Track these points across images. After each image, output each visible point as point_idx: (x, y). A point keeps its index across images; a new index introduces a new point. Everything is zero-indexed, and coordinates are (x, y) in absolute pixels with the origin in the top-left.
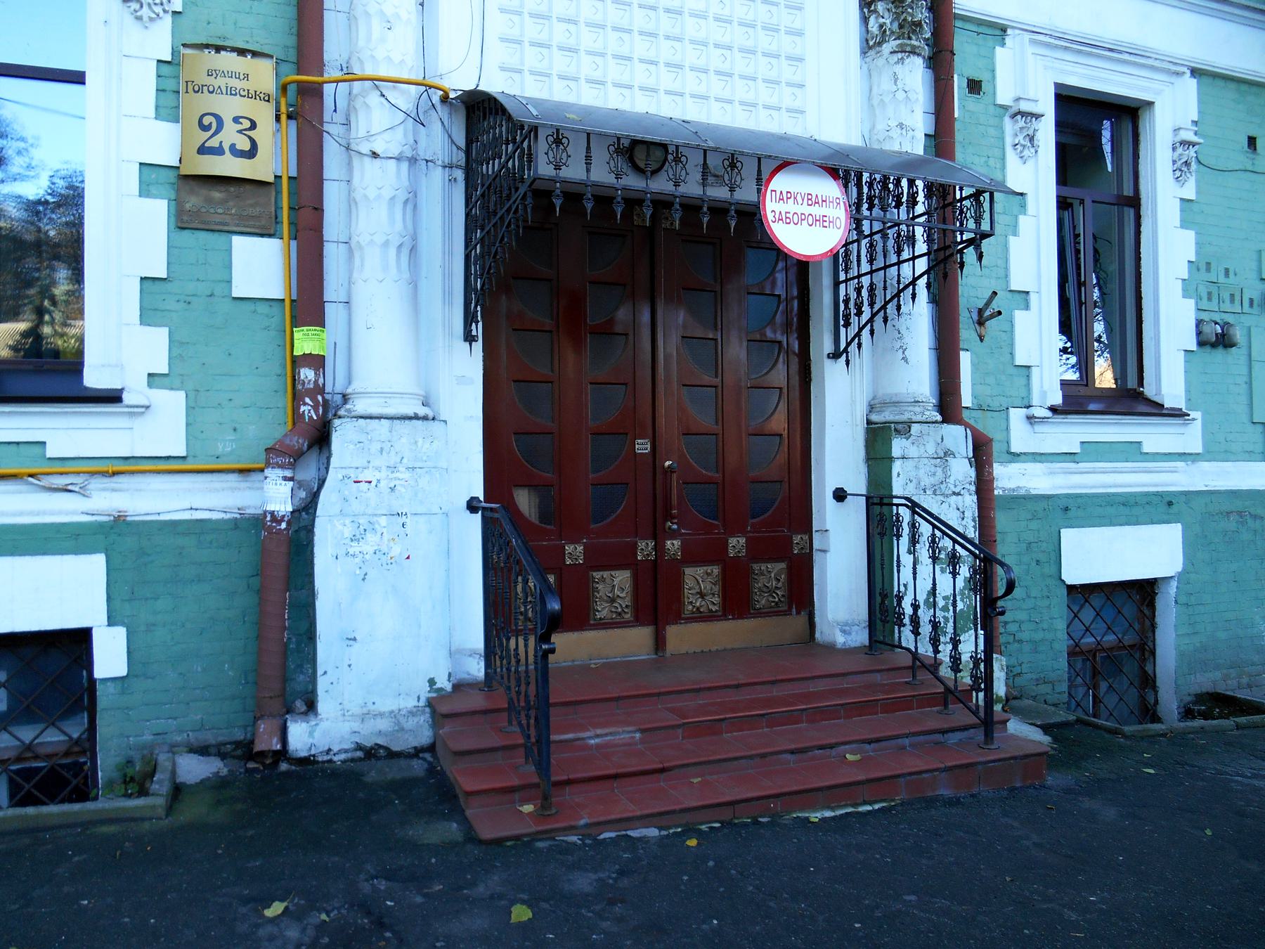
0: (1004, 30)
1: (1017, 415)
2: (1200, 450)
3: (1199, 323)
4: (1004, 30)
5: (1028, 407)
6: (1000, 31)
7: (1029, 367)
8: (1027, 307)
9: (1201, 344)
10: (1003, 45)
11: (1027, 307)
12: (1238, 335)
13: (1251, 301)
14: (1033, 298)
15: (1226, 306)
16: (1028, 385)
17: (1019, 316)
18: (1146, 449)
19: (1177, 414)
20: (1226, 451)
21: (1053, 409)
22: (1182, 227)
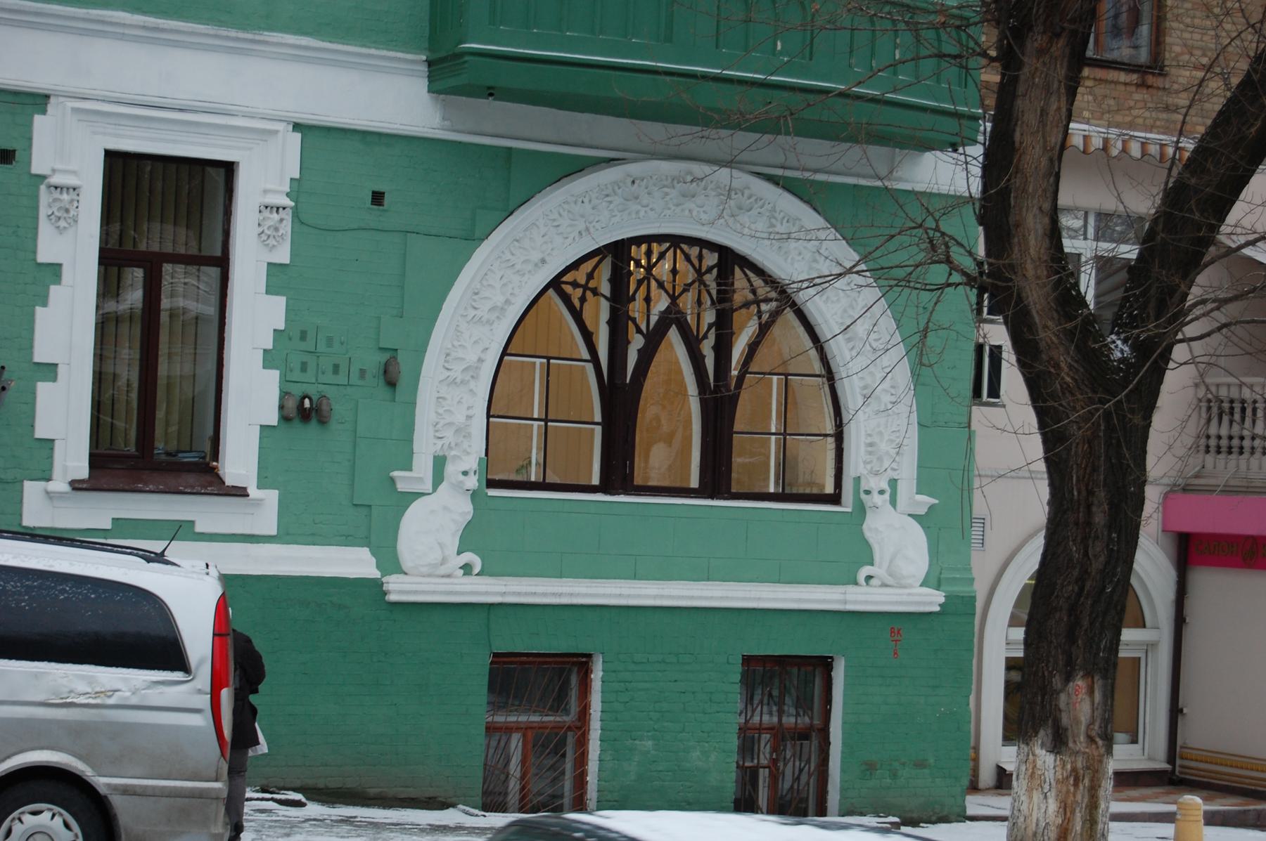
0: (47, 97)
1: (32, 490)
2: (274, 532)
3: (284, 395)
4: (47, 97)
5: (49, 479)
6: (39, 101)
7: (53, 441)
8: (54, 379)
9: (285, 418)
10: (44, 112)
11: (54, 379)
12: (339, 409)
13: (362, 373)
14: (61, 370)
15: (329, 378)
16: (51, 457)
17: (43, 388)
18: (199, 528)
19: (241, 492)
20: (313, 534)
21: (76, 486)
22: (267, 293)
